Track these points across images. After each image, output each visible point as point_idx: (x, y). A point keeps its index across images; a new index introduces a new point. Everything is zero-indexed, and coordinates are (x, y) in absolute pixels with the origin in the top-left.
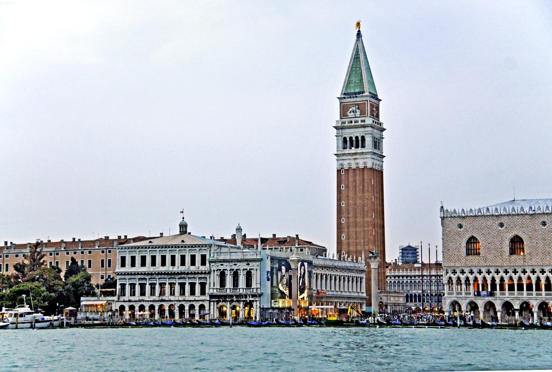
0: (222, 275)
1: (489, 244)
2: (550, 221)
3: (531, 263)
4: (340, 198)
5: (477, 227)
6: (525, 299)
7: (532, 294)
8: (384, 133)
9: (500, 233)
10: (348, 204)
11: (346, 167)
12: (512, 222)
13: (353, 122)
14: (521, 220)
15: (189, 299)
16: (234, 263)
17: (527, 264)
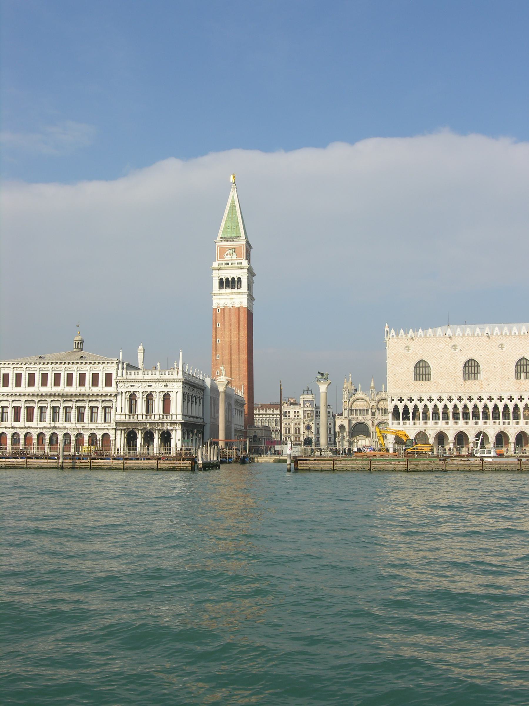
0: (132, 398)
1: (441, 368)
2: (509, 344)
3: (489, 389)
4: (216, 336)
5: (427, 350)
6: (482, 428)
7: (509, 423)
8: (254, 278)
9: (454, 356)
10: (223, 341)
11: (222, 306)
12: (467, 345)
13: (230, 264)
14: (477, 343)
15: (90, 427)
16: (148, 384)
17: (484, 390)
